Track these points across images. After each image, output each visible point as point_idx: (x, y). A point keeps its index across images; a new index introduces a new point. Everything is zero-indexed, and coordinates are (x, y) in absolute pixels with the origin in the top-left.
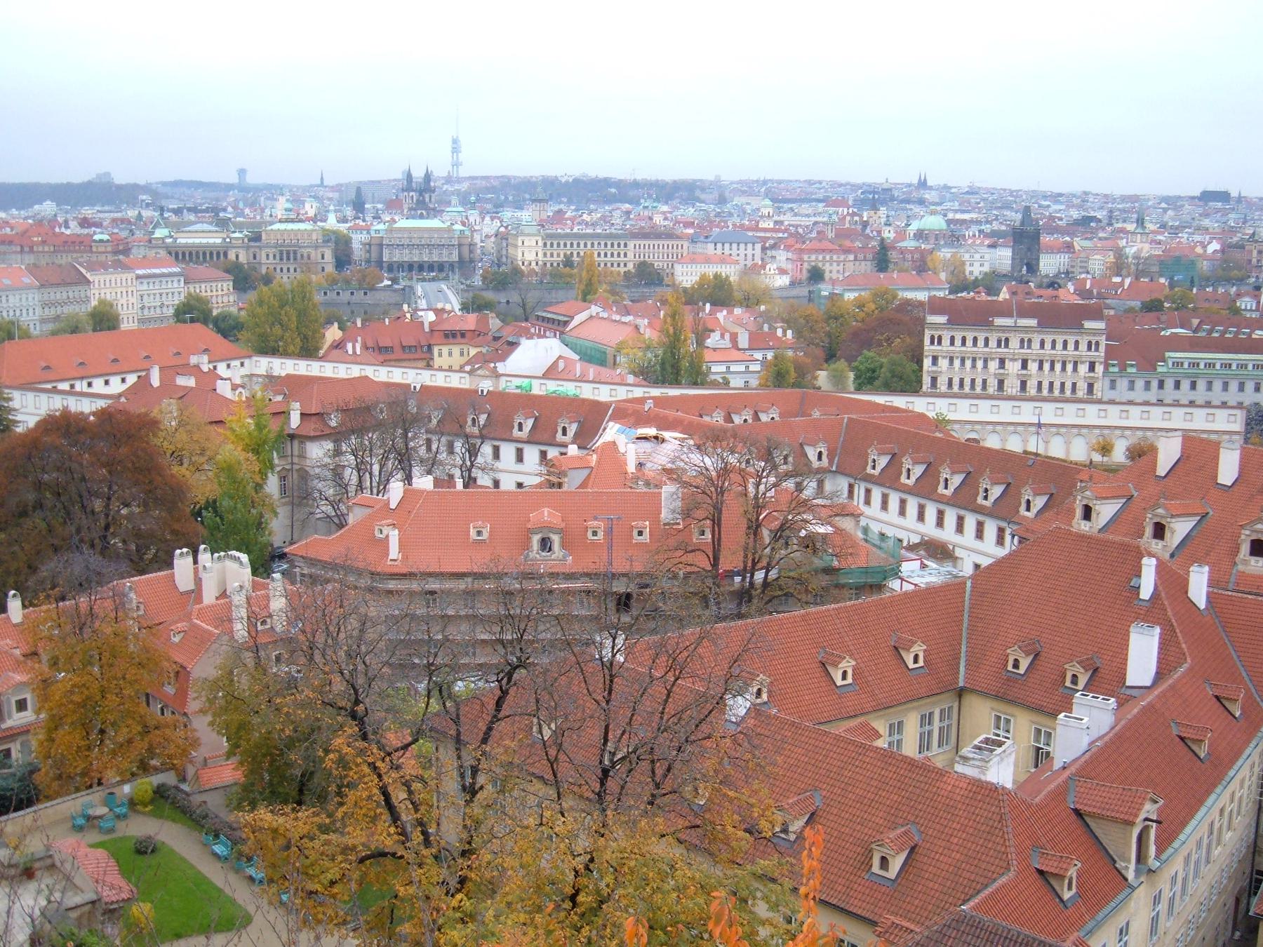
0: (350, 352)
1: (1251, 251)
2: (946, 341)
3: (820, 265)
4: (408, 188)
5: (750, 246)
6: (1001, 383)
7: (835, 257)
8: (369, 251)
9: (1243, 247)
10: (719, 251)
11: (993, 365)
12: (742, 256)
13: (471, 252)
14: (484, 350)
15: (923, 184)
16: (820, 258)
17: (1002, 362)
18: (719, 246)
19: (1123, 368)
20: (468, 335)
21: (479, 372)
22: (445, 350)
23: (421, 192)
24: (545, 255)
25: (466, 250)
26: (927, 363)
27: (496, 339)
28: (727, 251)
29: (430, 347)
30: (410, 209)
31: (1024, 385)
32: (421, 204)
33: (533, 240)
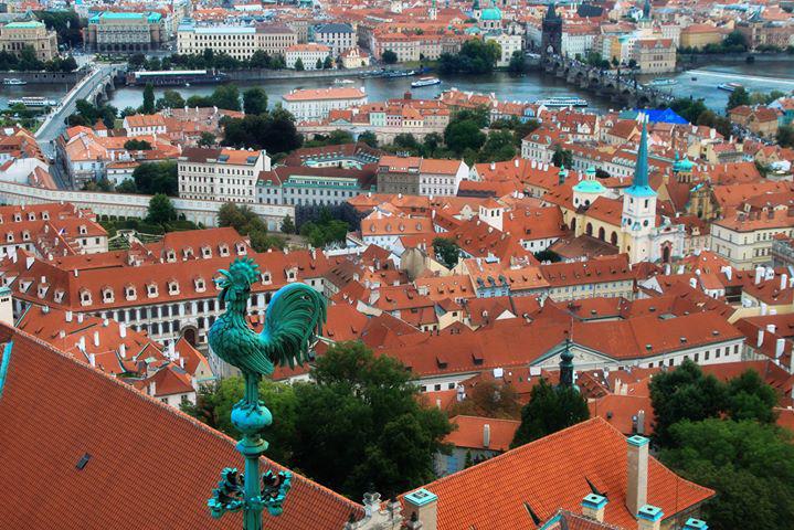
1: (751, 29)
2: (187, 169)
3: (393, 50)
6: (212, 189)
7: (404, 44)
9: (747, 25)
11: (208, 180)
12: (336, 42)
13: (161, 35)
16: (394, 44)
17: (212, 180)
18: (325, 35)
19: (265, 183)
24: (197, 45)
26: (180, 178)
31: (222, 189)
33: (188, 34)
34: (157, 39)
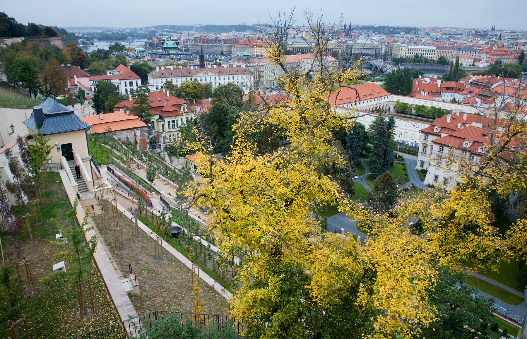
0: (423, 95)
4: (345, 29)
5: (474, 52)
7: (506, 57)
8: (348, 50)
10: (464, 54)
14: (469, 96)
15: (493, 29)
18: (464, 52)
20: (454, 89)
21: (492, 109)
22: (446, 94)
23: (349, 30)
24: (408, 53)
25: (377, 50)
27: (470, 92)
28: (466, 54)
29: (440, 93)
30: (345, 36)
32: (348, 34)
33: (405, 48)
34: (378, 52)
